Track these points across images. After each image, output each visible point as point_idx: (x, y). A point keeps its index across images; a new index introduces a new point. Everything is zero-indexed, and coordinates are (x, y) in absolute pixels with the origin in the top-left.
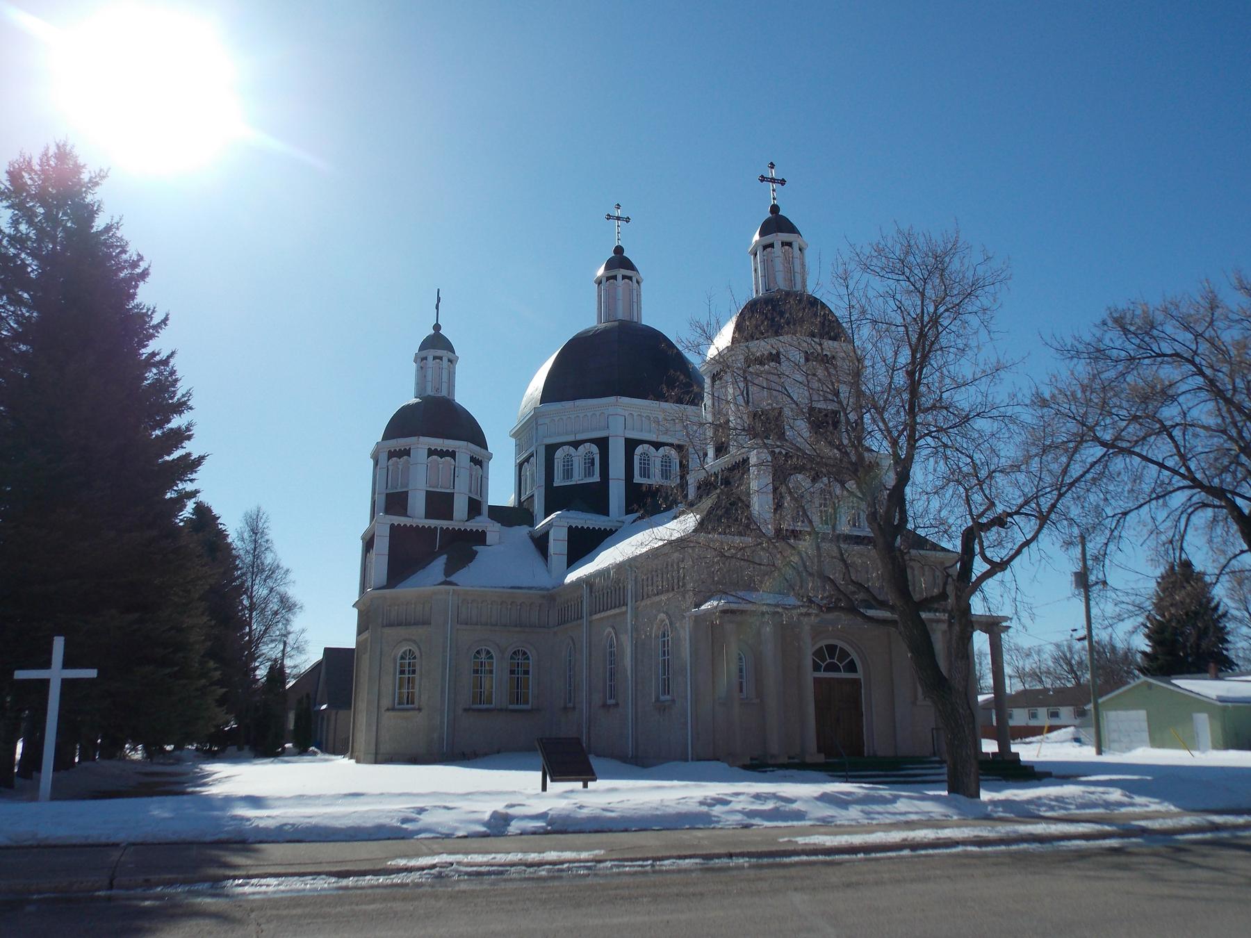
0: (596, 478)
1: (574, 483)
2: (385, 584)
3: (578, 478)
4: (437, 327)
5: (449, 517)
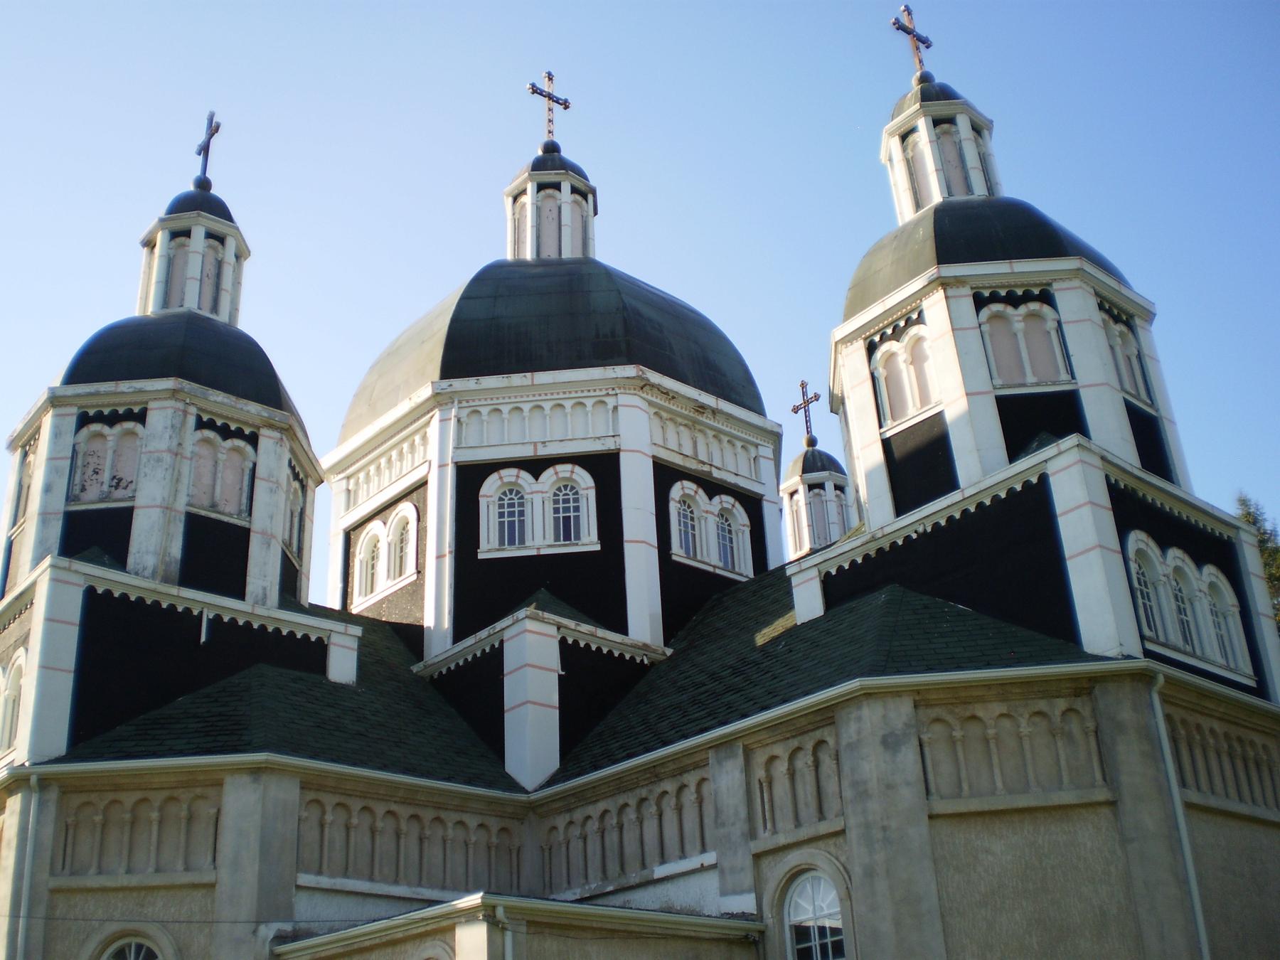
0: (589, 540)
1: (534, 553)
5: (239, 592)
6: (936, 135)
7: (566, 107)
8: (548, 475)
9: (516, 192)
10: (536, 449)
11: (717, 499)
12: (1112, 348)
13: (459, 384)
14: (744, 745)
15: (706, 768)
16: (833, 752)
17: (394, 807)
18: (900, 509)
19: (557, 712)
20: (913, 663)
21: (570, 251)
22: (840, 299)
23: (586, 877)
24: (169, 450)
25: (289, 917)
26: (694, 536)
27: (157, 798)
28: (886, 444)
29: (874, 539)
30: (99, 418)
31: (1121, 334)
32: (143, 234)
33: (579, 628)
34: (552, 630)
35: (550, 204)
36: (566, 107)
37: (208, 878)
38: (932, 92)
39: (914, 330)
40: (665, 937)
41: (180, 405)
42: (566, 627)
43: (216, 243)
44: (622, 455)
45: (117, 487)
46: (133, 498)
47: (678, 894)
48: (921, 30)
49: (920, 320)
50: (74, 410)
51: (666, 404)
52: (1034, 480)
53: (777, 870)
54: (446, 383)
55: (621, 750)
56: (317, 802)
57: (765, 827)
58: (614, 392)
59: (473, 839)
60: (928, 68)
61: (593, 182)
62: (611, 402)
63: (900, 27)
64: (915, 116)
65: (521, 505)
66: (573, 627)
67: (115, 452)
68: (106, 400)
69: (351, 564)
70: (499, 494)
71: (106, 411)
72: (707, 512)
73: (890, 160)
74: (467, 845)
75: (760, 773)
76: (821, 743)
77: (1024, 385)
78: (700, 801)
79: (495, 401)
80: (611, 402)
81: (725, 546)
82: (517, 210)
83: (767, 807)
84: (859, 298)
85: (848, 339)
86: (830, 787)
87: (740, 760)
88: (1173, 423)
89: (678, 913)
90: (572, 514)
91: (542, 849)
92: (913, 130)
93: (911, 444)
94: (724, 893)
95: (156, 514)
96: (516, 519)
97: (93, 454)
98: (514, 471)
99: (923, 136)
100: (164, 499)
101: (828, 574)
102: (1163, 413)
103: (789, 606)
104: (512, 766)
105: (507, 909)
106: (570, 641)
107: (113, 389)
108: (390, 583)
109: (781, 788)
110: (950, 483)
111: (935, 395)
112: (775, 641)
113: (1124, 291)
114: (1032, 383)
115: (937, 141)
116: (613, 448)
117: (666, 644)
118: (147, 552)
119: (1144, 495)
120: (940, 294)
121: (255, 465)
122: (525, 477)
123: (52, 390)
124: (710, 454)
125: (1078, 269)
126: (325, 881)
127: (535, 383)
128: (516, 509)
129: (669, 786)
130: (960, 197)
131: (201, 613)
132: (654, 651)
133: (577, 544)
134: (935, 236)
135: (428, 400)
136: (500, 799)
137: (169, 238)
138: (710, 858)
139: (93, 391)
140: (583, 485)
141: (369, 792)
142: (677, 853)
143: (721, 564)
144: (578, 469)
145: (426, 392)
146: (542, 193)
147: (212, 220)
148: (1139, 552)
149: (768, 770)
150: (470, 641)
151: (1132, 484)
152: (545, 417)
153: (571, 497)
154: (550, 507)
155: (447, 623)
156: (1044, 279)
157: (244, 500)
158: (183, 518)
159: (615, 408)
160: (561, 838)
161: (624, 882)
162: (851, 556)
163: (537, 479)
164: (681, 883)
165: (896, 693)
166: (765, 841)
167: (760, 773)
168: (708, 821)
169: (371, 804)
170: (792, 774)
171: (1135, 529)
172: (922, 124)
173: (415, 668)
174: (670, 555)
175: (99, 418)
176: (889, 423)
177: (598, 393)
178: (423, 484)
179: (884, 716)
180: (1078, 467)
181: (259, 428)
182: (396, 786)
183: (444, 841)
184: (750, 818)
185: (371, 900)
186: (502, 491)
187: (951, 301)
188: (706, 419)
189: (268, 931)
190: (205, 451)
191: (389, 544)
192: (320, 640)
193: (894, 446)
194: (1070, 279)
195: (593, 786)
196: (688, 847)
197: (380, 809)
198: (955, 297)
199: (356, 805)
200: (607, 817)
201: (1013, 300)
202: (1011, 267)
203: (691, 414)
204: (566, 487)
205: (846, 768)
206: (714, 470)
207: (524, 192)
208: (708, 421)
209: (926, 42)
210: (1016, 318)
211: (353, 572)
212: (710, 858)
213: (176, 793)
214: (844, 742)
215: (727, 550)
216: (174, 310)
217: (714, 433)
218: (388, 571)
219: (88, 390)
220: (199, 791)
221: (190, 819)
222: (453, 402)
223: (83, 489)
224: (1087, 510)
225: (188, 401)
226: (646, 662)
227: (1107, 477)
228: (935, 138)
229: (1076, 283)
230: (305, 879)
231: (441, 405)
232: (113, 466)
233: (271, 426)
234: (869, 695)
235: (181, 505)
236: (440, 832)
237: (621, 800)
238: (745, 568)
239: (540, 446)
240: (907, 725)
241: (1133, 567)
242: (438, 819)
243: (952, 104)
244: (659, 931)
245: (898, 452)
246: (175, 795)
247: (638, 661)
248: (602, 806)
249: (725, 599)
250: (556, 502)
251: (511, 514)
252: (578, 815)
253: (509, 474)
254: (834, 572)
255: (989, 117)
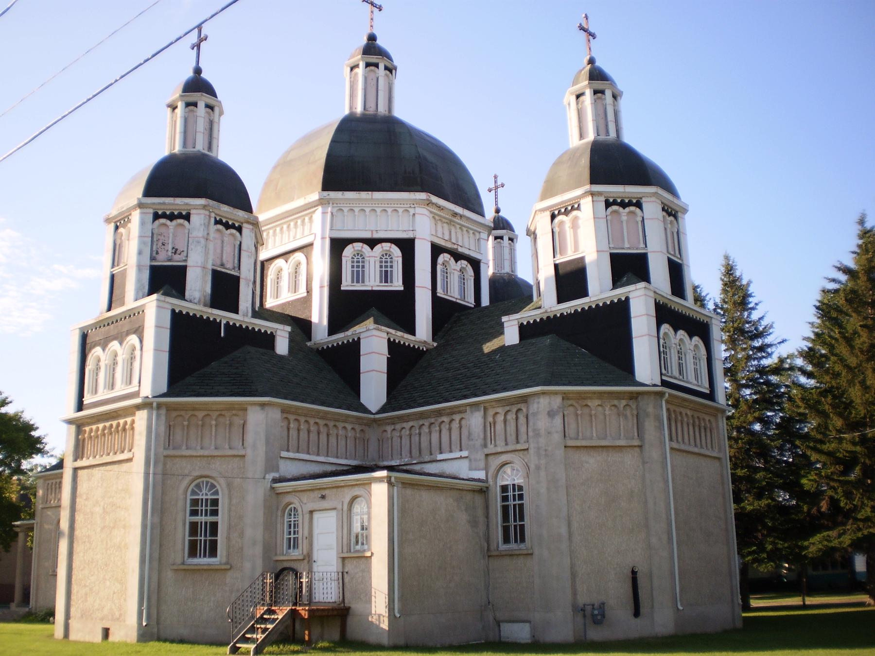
0: (397, 284)
1: (369, 289)
2: (165, 391)
3: (373, 282)
4: (198, 71)
6: (595, 99)
7: (380, 10)
8: (378, 248)
9: (353, 65)
10: (372, 234)
11: (459, 262)
12: (666, 229)
13: (333, 195)
14: (484, 407)
15: (465, 413)
16: (525, 414)
17: (317, 420)
18: (560, 301)
19: (386, 375)
20: (564, 379)
21: (382, 110)
22: (539, 186)
23: (401, 455)
24: (203, 237)
25: (277, 471)
26: (447, 281)
27: (215, 414)
28: (556, 266)
29: (546, 312)
30: (164, 216)
31: (671, 222)
32: (169, 100)
33: (396, 334)
34: (385, 335)
35: (372, 76)
36: (380, 10)
37: (242, 453)
38: (597, 75)
39: (575, 213)
40: (451, 489)
41: (207, 213)
42: (391, 334)
43: (210, 110)
44: (416, 240)
45: (175, 253)
46: (186, 261)
47: (449, 468)
48: (592, 30)
49: (578, 208)
50: (151, 211)
51: (439, 213)
52: (623, 299)
53: (495, 462)
54: (326, 193)
55: (421, 398)
56: (286, 418)
57: (491, 443)
58: (413, 206)
59: (350, 435)
60: (594, 55)
61: (396, 63)
62: (412, 211)
63: (582, 28)
64: (585, 87)
65: (363, 262)
66: (394, 333)
67: (173, 234)
68: (168, 207)
69: (265, 280)
70: (352, 255)
71: (168, 213)
72: (454, 270)
73: (569, 104)
74: (346, 437)
75: (490, 419)
76: (519, 410)
77: (623, 249)
78: (461, 427)
79: (351, 205)
80: (412, 211)
81: (461, 286)
82: (353, 76)
83: (492, 434)
84: (549, 191)
85: (543, 210)
86: (523, 429)
87: (482, 413)
88: (688, 266)
89: (447, 477)
90: (389, 269)
91: (379, 440)
92: (582, 94)
93: (569, 269)
94: (471, 469)
95: (199, 270)
96: (360, 269)
97: (161, 235)
98: (360, 244)
99: (588, 98)
100: (202, 263)
101: (522, 324)
102: (685, 262)
103: (502, 333)
104: (363, 400)
105: (396, 478)
106: (392, 340)
107: (173, 202)
108: (290, 295)
109: (500, 426)
110: (585, 294)
111: (582, 247)
112: (494, 352)
113: (675, 201)
114: (628, 247)
115: (595, 102)
116: (412, 236)
117: (434, 340)
118: (195, 290)
119: (671, 306)
120: (589, 199)
121: (241, 243)
122: (366, 248)
123: (138, 199)
124: (457, 240)
125: (656, 193)
126: (291, 455)
127: (374, 198)
128: (361, 264)
129: (446, 419)
130: (602, 137)
131: (221, 321)
132: (429, 344)
133: (391, 286)
134: (590, 167)
135: (316, 200)
136: (361, 417)
137: (184, 107)
138: (465, 453)
139: (162, 202)
140: (396, 255)
141: (308, 414)
142: (448, 449)
143: (459, 297)
144: (393, 246)
145: (315, 196)
146: (368, 68)
147: (209, 98)
148: (665, 334)
149: (494, 418)
150: (340, 336)
151: (666, 301)
152: (377, 216)
153: (389, 260)
154: (378, 265)
155: (325, 322)
156: (639, 196)
157: (236, 261)
158: (210, 272)
159: (414, 214)
160: (389, 436)
161: (422, 460)
162: (535, 318)
163: (372, 249)
164: (450, 462)
165: (556, 393)
166: (491, 449)
167: (490, 419)
168: (464, 437)
169: (308, 419)
170: (505, 421)
171: (664, 323)
172: (588, 93)
173: (309, 344)
174: (436, 293)
175: (164, 216)
176: (558, 256)
177: (405, 206)
178: (311, 245)
179: (550, 403)
180: (643, 298)
181: (242, 223)
182: (318, 411)
183: (337, 435)
184: (485, 439)
185: (308, 463)
186: (354, 253)
187: (595, 203)
188: (457, 220)
189: (270, 476)
190: (217, 235)
191: (289, 274)
192: (272, 333)
193: (560, 268)
194: (651, 197)
195: (409, 415)
196: (453, 447)
197: (312, 421)
198: (596, 201)
199: (302, 419)
200: (413, 429)
201: (623, 205)
202: (625, 189)
203: (450, 218)
204: (386, 254)
205: (531, 423)
206: (459, 247)
207: (357, 66)
208: (457, 221)
209: (593, 35)
210: (624, 214)
211: (266, 285)
212: (465, 453)
213: (223, 413)
214: (531, 412)
215: (463, 290)
216: (190, 150)
217: (459, 226)
218: (289, 287)
219: (159, 201)
220: (234, 412)
221: (231, 425)
222: (329, 204)
223: (157, 253)
224: (645, 318)
225: (211, 210)
226: (425, 349)
227: (655, 300)
228: (594, 101)
229: (653, 199)
230: (284, 454)
231: (323, 204)
232: (173, 242)
233: (248, 222)
234: (544, 393)
235: (210, 267)
236: (335, 431)
237: (421, 422)
238: (470, 301)
239: (374, 232)
240: (559, 407)
241: (662, 341)
242: (335, 426)
243: (604, 83)
244: (448, 486)
245: (561, 271)
246: (223, 414)
247: (421, 349)
248: (411, 424)
249: (462, 318)
250: (381, 262)
251: (358, 267)
252: (398, 427)
253: (358, 246)
254: (525, 323)
255: (622, 90)
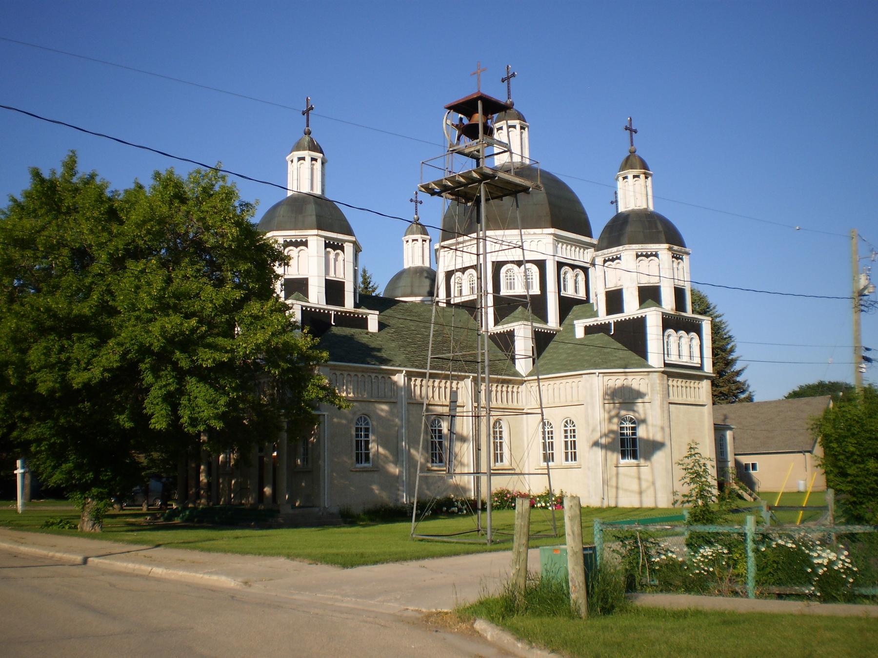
0: (536, 290)
90: (530, 280)
122: (515, 267)
251: (510, 279)
